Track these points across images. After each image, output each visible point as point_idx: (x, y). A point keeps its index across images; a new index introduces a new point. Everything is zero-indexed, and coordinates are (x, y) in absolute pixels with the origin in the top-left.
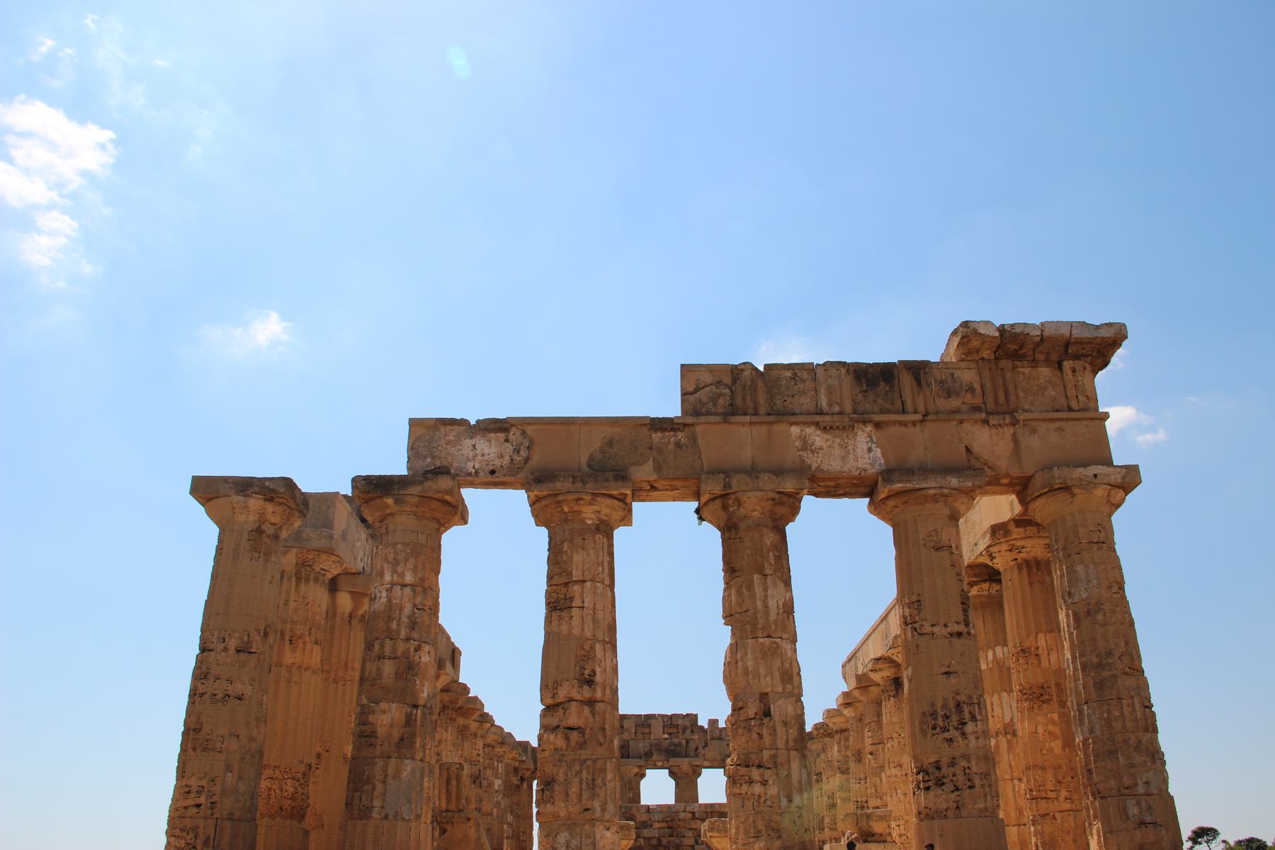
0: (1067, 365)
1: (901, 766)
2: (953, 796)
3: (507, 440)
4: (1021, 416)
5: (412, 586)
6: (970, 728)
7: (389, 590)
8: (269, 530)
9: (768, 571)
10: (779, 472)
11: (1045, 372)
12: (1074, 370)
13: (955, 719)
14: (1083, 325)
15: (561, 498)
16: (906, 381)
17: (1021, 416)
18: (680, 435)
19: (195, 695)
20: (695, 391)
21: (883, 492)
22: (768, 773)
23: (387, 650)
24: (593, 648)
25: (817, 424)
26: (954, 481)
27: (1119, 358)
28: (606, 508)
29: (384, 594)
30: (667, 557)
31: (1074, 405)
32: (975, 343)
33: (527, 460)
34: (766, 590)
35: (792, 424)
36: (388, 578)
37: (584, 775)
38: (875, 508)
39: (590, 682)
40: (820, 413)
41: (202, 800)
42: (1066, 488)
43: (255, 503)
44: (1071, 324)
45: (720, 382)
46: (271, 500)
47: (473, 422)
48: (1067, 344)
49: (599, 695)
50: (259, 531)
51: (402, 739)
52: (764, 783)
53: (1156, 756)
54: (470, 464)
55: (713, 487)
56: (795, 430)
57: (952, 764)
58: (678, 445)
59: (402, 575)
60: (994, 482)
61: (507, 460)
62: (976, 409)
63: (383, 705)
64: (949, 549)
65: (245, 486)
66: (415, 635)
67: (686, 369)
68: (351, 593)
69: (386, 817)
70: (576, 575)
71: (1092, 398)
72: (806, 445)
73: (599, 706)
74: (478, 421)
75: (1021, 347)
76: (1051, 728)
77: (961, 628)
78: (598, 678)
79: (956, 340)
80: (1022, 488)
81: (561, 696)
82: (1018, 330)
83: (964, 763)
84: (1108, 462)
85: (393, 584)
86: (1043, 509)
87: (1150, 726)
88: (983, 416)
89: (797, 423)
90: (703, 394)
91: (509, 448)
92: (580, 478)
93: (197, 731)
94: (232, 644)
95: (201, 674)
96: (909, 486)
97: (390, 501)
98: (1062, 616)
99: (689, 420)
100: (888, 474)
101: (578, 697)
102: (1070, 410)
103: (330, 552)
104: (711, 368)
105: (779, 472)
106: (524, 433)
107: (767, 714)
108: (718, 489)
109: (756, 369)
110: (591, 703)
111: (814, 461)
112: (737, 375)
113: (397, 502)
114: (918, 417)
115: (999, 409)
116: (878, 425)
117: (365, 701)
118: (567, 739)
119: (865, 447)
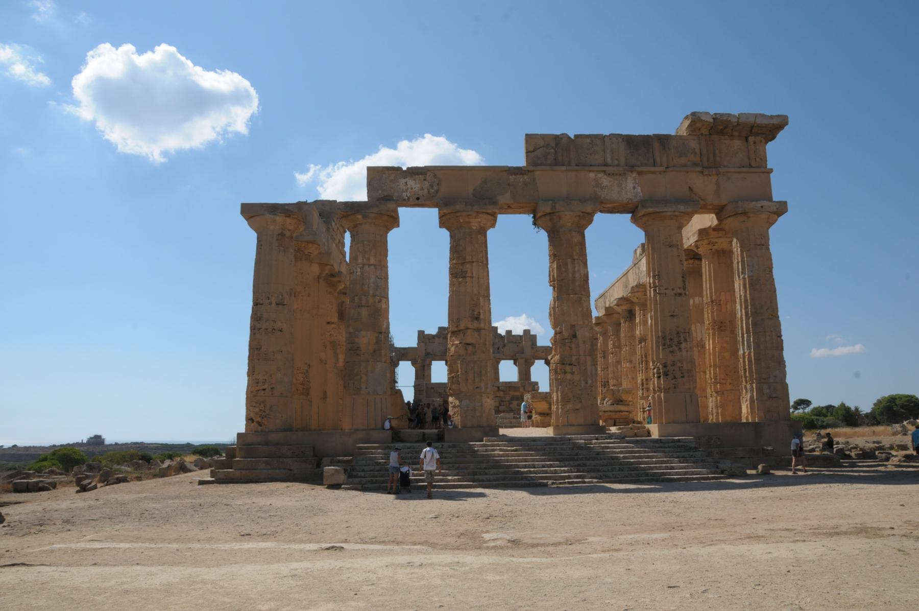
0: (751, 139)
1: (631, 362)
2: (673, 382)
3: (425, 180)
4: (722, 170)
5: (374, 265)
6: (683, 345)
7: (362, 268)
8: (288, 234)
9: (575, 257)
10: (583, 200)
11: (738, 143)
12: (755, 143)
13: (676, 342)
14: (763, 116)
15: (458, 214)
16: (657, 145)
17: (720, 170)
18: (526, 177)
19: (254, 329)
20: (534, 150)
21: (641, 212)
22: (575, 369)
23: (363, 302)
24: (479, 299)
25: (604, 172)
26: (682, 208)
27: (781, 135)
28: (484, 219)
29: (359, 270)
30: (517, 248)
31: (753, 164)
32: (698, 125)
33: (437, 192)
34: (574, 268)
35: (590, 171)
36: (360, 261)
37: (476, 369)
38: (634, 220)
39: (477, 319)
40: (606, 165)
41: (266, 386)
42: (744, 213)
43: (280, 219)
44: (756, 115)
45: (548, 146)
46: (289, 216)
47: (404, 169)
48: (752, 127)
49: (482, 326)
50: (282, 234)
51: (375, 351)
52: (573, 373)
53: (781, 363)
54: (404, 194)
55: (545, 208)
56: (592, 175)
57: (673, 365)
58: (525, 183)
59: (369, 259)
60: (704, 208)
61: (426, 191)
62: (695, 164)
63: (363, 333)
64: (677, 245)
65: (274, 209)
66: (378, 293)
67: (529, 137)
68: (320, 264)
69: (369, 393)
70: (468, 258)
71: (764, 160)
72: (598, 184)
73: (482, 332)
74: (408, 168)
75: (725, 128)
76: (725, 345)
77: (681, 291)
78: (482, 316)
79: (687, 123)
80: (719, 211)
81: (462, 326)
82: (725, 118)
83: (679, 364)
84: (770, 198)
85: (364, 265)
86: (730, 223)
87: (780, 347)
88: (700, 169)
89: (593, 171)
90: (538, 152)
91: (426, 184)
92: (465, 201)
93: (259, 349)
94: (273, 300)
95: (256, 318)
96: (657, 210)
97: (360, 217)
98: (738, 285)
99: (531, 168)
100: (644, 203)
101: (471, 327)
102: (751, 166)
103: (313, 242)
104: (543, 137)
105: (583, 200)
106: (435, 176)
107: (575, 336)
108: (548, 210)
109: (569, 138)
110: (478, 330)
111: (603, 194)
112: (558, 140)
113: (364, 217)
114: (663, 169)
115: (710, 164)
116: (640, 173)
117: (351, 330)
118: (466, 349)
119: (632, 186)
